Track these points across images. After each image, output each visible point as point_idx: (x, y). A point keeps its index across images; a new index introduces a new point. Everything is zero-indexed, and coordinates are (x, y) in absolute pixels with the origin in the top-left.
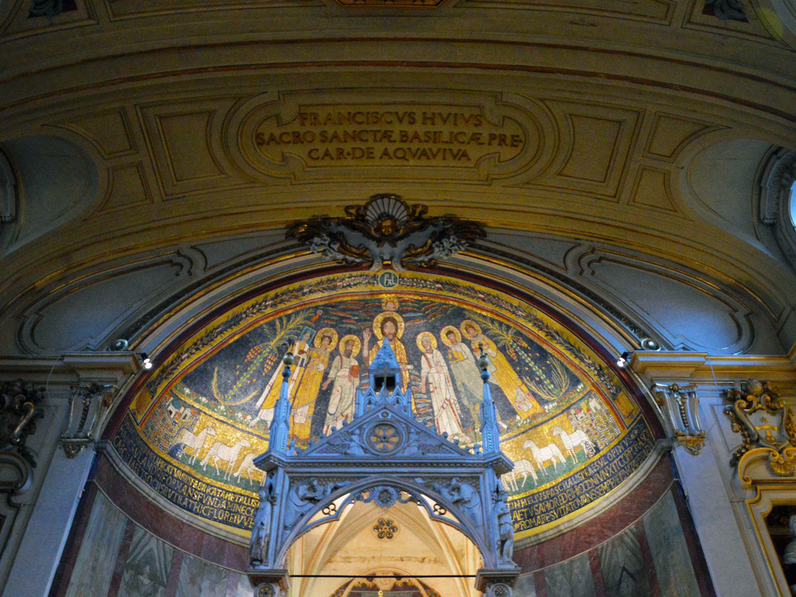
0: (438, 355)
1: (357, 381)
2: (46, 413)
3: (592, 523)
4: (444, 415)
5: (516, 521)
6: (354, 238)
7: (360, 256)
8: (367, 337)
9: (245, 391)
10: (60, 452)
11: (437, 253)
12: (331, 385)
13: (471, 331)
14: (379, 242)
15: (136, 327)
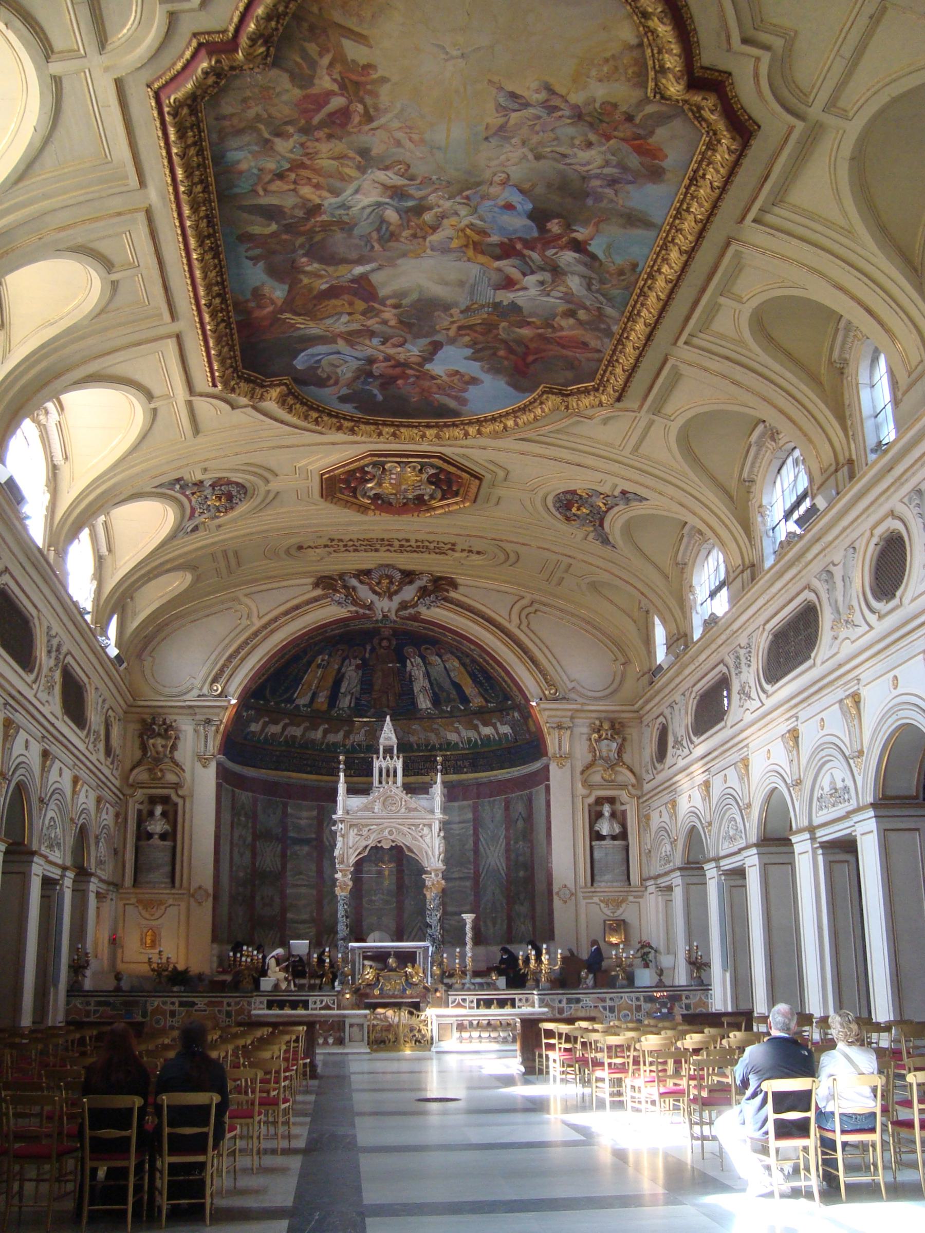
0: (419, 660)
1: (360, 672)
2: (181, 736)
4: (421, 696)
5: (465, 767)
8: (368, 648)
10: (198, 766)
12: (343, 675)
13: (443, 651)
15: (222, 670)
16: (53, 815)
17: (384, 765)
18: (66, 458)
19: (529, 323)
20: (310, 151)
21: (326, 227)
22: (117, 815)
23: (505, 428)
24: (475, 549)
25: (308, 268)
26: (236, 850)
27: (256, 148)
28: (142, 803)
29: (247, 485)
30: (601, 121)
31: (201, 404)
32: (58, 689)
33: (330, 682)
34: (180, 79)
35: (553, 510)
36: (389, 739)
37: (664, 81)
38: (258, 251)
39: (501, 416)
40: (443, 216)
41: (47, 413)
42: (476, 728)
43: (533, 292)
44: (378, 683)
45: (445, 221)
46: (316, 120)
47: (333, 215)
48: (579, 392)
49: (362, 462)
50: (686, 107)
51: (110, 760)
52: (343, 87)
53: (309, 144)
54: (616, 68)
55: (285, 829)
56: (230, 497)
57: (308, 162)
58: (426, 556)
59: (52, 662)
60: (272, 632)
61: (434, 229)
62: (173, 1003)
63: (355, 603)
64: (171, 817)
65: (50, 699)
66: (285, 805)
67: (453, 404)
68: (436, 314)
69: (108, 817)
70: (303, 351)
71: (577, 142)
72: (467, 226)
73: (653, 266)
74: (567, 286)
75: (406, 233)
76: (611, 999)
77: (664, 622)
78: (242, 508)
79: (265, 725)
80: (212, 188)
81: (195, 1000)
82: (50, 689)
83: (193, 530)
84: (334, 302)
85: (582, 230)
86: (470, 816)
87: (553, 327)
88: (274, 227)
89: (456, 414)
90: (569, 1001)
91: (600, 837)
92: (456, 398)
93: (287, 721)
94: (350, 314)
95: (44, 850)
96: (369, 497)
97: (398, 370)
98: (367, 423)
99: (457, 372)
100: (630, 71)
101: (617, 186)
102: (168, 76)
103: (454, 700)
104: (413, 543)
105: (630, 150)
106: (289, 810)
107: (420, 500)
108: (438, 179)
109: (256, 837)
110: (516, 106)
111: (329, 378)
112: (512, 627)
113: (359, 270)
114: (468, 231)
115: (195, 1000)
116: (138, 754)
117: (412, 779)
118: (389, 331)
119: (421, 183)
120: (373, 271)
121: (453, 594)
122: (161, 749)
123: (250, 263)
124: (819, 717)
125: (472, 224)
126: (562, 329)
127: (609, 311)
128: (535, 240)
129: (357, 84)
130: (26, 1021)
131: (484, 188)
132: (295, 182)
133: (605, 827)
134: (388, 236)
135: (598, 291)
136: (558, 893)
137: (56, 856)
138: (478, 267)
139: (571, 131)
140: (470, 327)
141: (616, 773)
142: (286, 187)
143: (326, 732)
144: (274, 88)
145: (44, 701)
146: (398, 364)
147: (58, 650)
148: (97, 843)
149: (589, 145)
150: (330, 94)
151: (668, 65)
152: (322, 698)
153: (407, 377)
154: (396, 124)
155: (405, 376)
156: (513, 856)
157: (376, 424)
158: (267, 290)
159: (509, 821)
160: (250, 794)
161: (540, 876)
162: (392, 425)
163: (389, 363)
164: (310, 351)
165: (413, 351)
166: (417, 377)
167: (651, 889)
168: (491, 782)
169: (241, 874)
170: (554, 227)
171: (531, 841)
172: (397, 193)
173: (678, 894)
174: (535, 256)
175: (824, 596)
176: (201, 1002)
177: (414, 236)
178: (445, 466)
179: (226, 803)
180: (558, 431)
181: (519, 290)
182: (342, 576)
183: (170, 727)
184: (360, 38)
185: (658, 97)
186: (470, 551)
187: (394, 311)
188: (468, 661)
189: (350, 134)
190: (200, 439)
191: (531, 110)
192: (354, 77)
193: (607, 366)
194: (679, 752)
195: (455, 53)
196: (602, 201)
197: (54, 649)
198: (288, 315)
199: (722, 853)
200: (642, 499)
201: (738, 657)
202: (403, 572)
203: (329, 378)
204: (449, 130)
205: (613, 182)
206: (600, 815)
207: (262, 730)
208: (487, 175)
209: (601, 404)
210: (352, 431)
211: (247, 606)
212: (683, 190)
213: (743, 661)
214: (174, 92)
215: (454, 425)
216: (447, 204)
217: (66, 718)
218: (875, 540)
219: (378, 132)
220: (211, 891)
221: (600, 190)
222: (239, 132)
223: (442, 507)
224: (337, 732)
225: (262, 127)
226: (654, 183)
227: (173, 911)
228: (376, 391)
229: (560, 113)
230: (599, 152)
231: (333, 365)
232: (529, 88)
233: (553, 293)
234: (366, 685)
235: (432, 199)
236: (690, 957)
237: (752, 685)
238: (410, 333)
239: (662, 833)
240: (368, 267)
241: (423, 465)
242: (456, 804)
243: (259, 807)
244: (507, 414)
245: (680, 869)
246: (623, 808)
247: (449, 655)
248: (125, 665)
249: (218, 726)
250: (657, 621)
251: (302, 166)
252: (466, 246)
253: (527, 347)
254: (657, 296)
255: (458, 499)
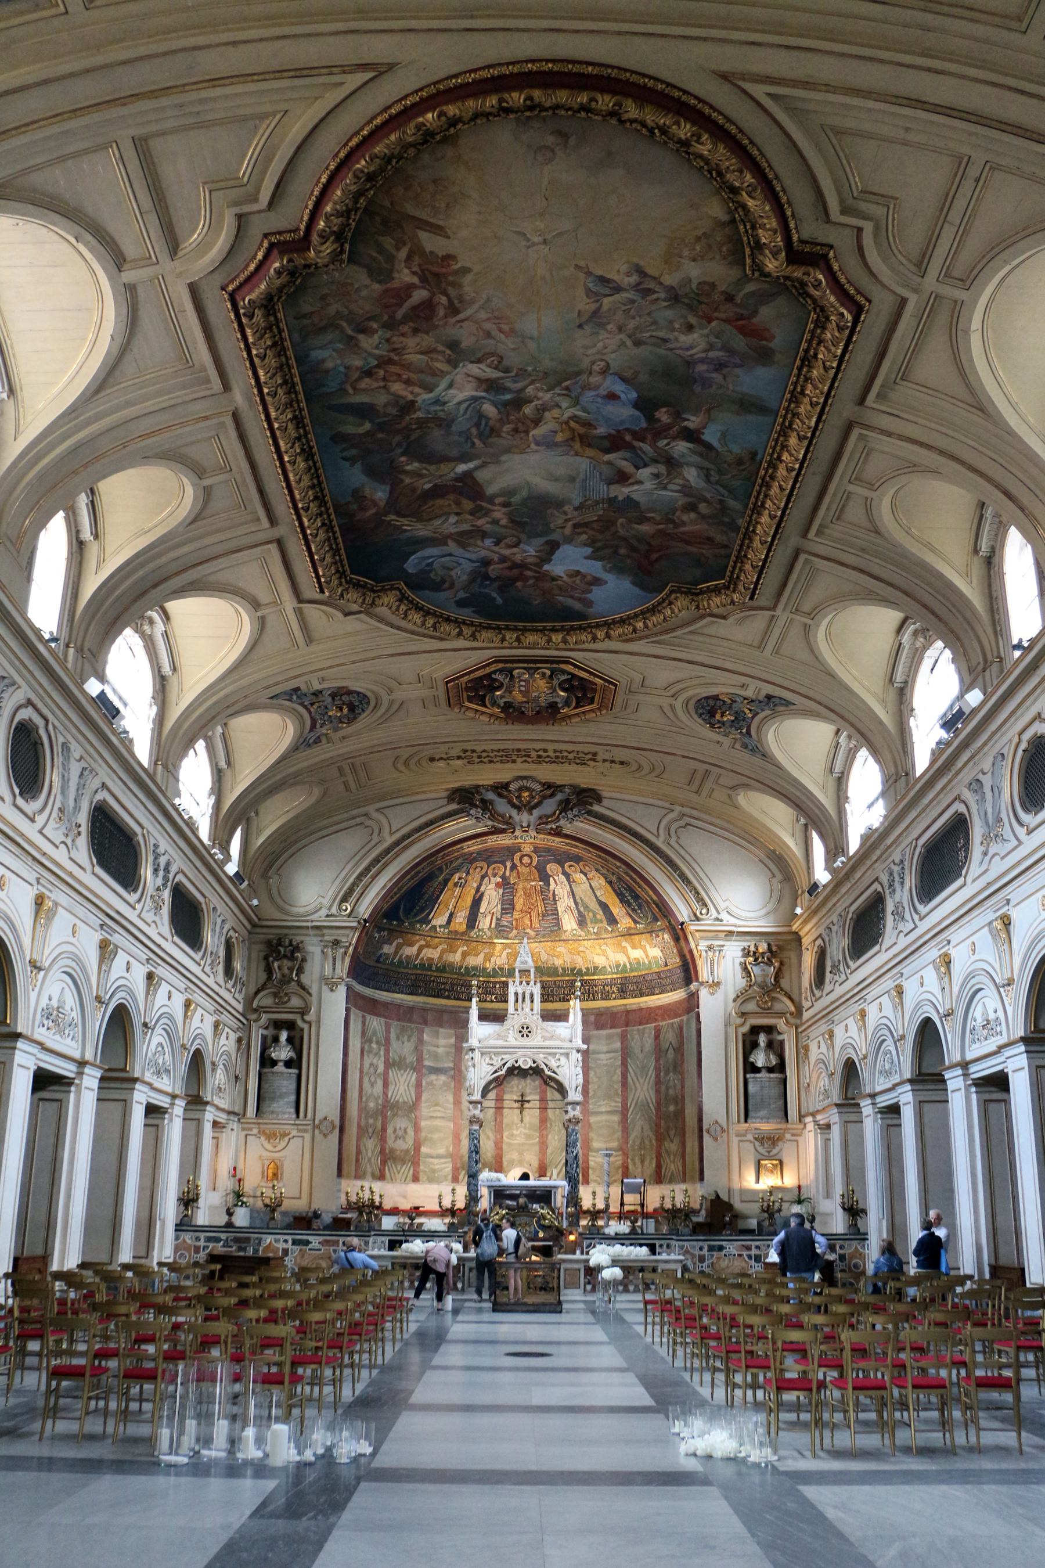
0: (563, 878)
1: (501, 891)
3: (659, 1008)
6: (501, 806)
7: (507, 823)
8: (509, 865)
9: (422, 910)
10: (325, 988)
11: (562, 822)
12: (482, 894)
14: (519, 809)
16: (161, 1040)
17: (520, 991)
18: (174, 669)
19: (648, 519)
20: (397, 346)
21: (422, 423)
22: (239, 1040)
23: (635, 630)
24: (617, 759)
25: (408, 468)
26: (366, 1079)
27: (340, 346)
28: (266, 1028)
29: (369, 694)
30: (700, 303)
31: (312, 612)
32: (166, 910)
33: (468, 901)
34: (254, 280)
35: (695, 716)
36: (525, 962)
37: (761, 258)
38: (354, 452)
39: (629, 617)
40: (543, 409)
41: (151, 622)
42: (624, 951)
43: (648, 485)
44: (519, 902)
45: (547, 414)
46: (400, 314)
47: (429, 412)
48: (709, 590)
49: (488, 670)
50: (788, 283)
51: (231, 983)
52: (423, 279)
53: (395, 339)
54: (710, 247)
55: (420, 1059)
56: (352, 708)
57: (396, 358)
58: (566, 766)
59: (159, 881)
60: (406, 848)
61: (537, 422)
62: (286, 1241)
63: (492, 818)
64: (297, 1042)
65: (157, 919)
66: (421, 1032)
67: (577, 606)
68: (549, 511)
69: (228, 1042)
70: (414, 553)
71: (677, 326)
72: (571, 418)
73: (772, 455)
74: (684, 478)
75: (507, 428)
76: (757, 1247)
77: (822, 836)
78: (365, 720)
79: (399, 947)
80: (299, 388)
81: (310, 1238)
82: (158, 908)
83: (315, 742)
84: (440, 502)
85: (693, 418)
86: (618, 1045)
87: (673, 522)
88: (368, 426)
89: (583, 617)
90: (711, 1249)
91: (756, 1070)
92: (579, 599)
93: (423, 943)
94: (457, 514)
95: (148, 1076)
96: (499, 706)
97: (515, 571)
98: (489, 627)
99: (578, 573)
100: (724, 249)
101: (725, 371)
102: (242, 277)
103: (601, 921)
104: (551, 754)
105: (735, 331)
106: (425, 1037)
107: (553, 707)
108: (535, 370)
109: (388, 1065)
110: (607, 291)
111: (443, 581)
112: (659, 843)
113: (462, 468)
114: (572, 424)
115: (310, 1238)
116: (263, 977)
117: (550, 1006)
118: (503, 530)
119: (517, 375)
120: (477, 468)
121: (596, 808)
122: (286, 971)
123: (348, 464)
124: (969, 941)
125: (575, 416)
126: (684, 524)
127: (732, 503)
128: (646, 430)
129: (437, 275)
130: (125, 1256)
131: (584, 377)
132: (384, 379)
133: (760, 1059)
134: (488, 431)
135: (717, 482)
136: (708, 1131)
137: (165, 1084)
138: (588, 461)
139: (669, 314)
140: (586, 525)
141: (773, 999)
142: (376, 385)
143: (465, 955)
144: (352, 284)
145: (149, 921)
146: (515, 565)
147: (167, 870)
148: (213, 1070)
149: (690, 328)
150: (411, 287)
151: (764, 240)
152: (461, 920)
153: (525, 579)
154: (483, 315)
155: (522, 578)
156: (663, 1088)
157: (498, 628)
158: (367, 492)
159: (659, 1051)
160: (383, 1020)
161: (690, 1111)
162: (516, 629)
163: (506, 565)
164: (419, 554)
165: (529, 551)
166: (537, 579)
167: (810, 1126)
168: (641, 1009)
169: (372, 1105)
170: (663, 416)
171: (682, 1074)
172: (491, 386)
173: (836, 1132)
174: (647, 448)
175: (974, 808)
176: (315, 1241)
177: (516, 430)
178: (576, 672)
179: (355, 1027)
180: (691, 632)
181: (632, 484)
182: (478, 787)
183: (297, 948)
184: (437, 230)
185: (757, 274)
186: (612, 762)
187: (504, 510)
188: (614, 879)
189: (436, 327)
190: (313, 648)
191: (625, 295)
192: (435, 269)
193: (735, 563)
194: (836, 978)
195: (536, 239)
196: (711, 386)
197: (162, 867)
198: (394, 517)
199: (878, 1089)
200: (788, 703)
201: (891, 874)
202: (544, 785)
203: (443, 581)
204: (539, 319)
205: (720, 366)
206: (755, 1045)
207: (396, 952)
208: (586, 363)
209: (733, 602)
210: (474, 637)
211: (378, 822)
212: (795, 371)
213: (897, 879)
214: (249, 293)
215: (581, 628)
216: (547, 396)
217: (176, 939)
218: (1024, 746)
219: (464, 324)
220: (337, 1123)
221: (706, 375)
222: (323, 330)
223: (577, 715)
224: (477, 955)
225: (345, 324)
226: (764, 365)
227: (296, 1143)
228: (494, 595)
229: (655, 296)
230: (702, 336)
231: (444, 568)
232: (618, 271)
233: (671, 486)
234: (508, 907)
235: (530, 390)
236: (843, 1203)
237: (906, 904)
238: (523, 532)
239: (821, 1065)
240: (471, 465)
241: (553, 672)
242: (604, 1032)
243: (393, 1035)
244: (636, 616)
245: (837, 1105)
246: (780, 1038)
247: (594, 873)
248: (246, 883)
249: (348, 948)
250: (815, 836)
251: (390, 362)
252: (573, 439)
253: (649, 544)
254: (780, 486)
255: (594, 706)
